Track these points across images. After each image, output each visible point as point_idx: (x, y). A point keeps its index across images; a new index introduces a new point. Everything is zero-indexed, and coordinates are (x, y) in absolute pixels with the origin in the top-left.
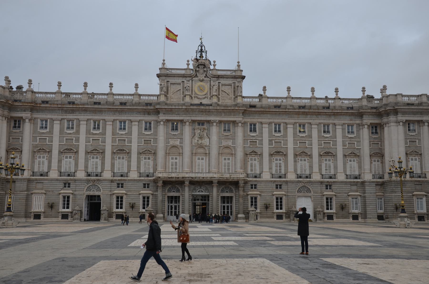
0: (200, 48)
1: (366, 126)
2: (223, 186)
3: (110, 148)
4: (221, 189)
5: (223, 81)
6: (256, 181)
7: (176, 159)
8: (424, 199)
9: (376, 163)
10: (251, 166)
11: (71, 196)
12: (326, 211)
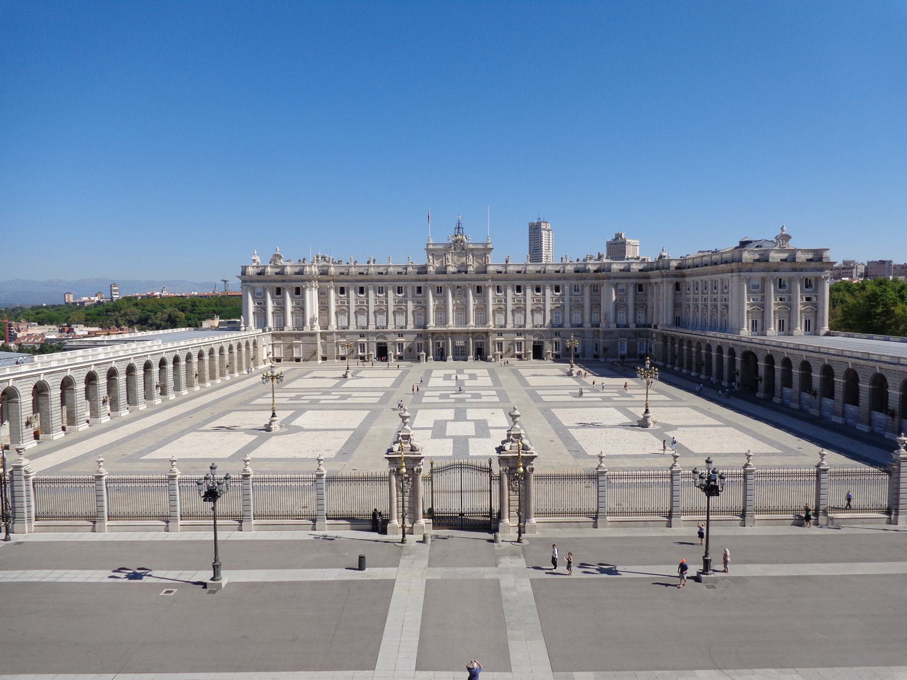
0: (458, 225)
1: (588, 286)
2: (477, 334)
3: (393, 307)
4: (475, 337)
5: (475, 252)
6: (501, 331)
7: (441, 314)
8: (626, 343)
9: (596, 314)
10: (498, 319)
11: (366, 344)
12: (554, 352)
